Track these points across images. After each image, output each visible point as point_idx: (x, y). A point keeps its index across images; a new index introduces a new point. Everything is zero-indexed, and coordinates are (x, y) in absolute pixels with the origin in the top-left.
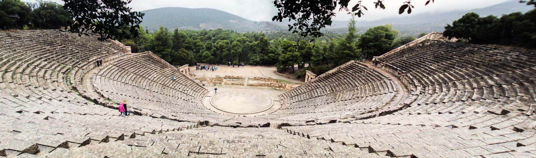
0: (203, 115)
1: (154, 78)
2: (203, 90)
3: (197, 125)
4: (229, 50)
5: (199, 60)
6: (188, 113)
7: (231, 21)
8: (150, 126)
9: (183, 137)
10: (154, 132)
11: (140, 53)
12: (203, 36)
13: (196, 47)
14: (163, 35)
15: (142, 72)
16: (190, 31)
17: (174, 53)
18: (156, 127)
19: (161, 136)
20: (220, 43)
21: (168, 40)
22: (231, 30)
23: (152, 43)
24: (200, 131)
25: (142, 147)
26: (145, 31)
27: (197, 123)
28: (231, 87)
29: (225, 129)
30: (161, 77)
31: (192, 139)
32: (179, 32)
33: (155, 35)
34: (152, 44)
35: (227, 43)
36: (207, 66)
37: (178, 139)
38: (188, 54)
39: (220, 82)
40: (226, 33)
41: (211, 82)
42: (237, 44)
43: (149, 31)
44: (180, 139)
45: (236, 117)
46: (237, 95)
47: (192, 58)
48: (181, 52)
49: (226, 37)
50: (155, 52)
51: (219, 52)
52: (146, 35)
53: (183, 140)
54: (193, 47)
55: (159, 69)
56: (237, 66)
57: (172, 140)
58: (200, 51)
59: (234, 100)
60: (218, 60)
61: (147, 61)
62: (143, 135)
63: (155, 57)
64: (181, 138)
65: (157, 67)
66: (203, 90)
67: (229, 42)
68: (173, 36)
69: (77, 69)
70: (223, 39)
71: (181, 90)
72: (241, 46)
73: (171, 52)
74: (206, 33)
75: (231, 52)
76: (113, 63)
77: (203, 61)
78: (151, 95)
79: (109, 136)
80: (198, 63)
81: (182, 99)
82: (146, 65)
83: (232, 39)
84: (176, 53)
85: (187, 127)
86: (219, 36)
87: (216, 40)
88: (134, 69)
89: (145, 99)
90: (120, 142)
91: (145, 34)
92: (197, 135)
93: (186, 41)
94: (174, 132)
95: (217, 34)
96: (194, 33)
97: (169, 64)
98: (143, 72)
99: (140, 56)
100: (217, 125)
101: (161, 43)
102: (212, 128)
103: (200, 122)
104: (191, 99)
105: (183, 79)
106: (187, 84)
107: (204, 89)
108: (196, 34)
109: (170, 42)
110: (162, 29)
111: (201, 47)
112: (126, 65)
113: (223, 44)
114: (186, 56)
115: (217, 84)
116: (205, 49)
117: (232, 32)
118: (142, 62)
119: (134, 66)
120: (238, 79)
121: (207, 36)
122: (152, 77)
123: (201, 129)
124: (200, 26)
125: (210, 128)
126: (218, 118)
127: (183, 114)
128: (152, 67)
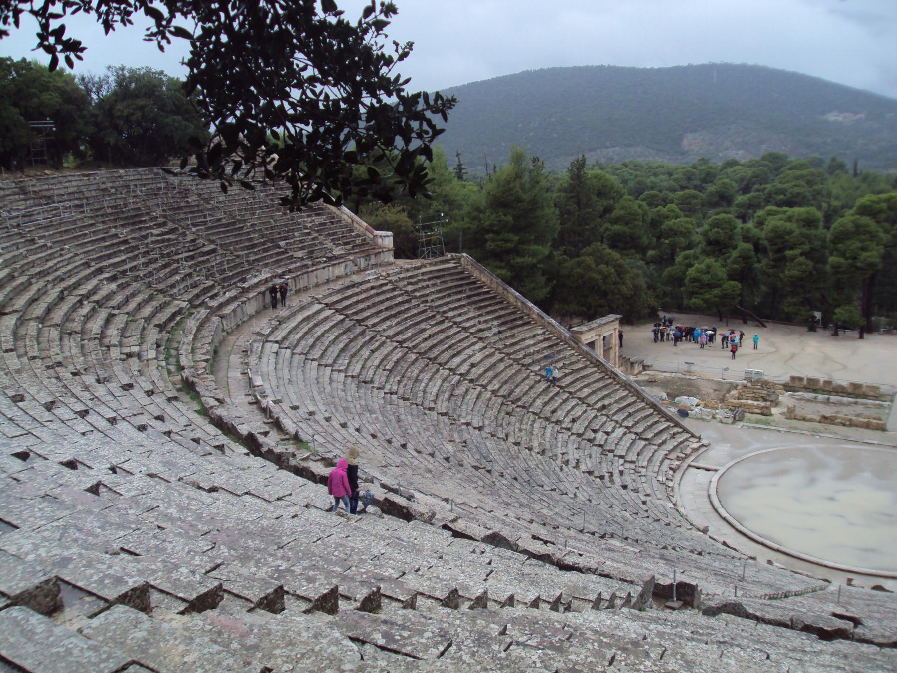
0: (670, 553)
1: (473, 366)
2: (680, 438)
3: (642, 596)
4: (815, 255)
5: (668, 299)
6: (603, 537)
7: (832, 117)
8: (441, 571)
9: (575, 641)
10: (452, 600)
11: (425, 261)
12: (695, 188)
13: (659, 238)
14: (522, 187)
15: (425, 340)
16: (637, 167)
17: (560, 263)
18: (462, 577)
19: (481, 622)
20: (773, 222)
21: (542, 208)
22: (828, 161)
23: (474, 219)
24: (652, 626)
25: (400, 657)
26: (451, 169)
27: (640, 589)
28: (815, 432)
29: (774, 639)
30: (502, 366)
31: (613, 658)
32: (590, 173)
33: (490, 187)
34: (476, 222)
35: (809, 223)
36: (703, 327)
37: (552, 646)
38: (620, 271)
39: (763, 404)
40: (804, 172)
41: (722, 400)
42: (857, 226)
43: (469, 171)
44: (560, 649)
45: (832, 588)
46: (843, 477)
47: (636, 288)
48: (589, 260)
49: (805, 190)
50: (484, 257)
51: (765, 261)
52: (455, 189)
53: (572, 657)
54: (645, 240)
55: (495, 330)
56: (856, 334)
57: (524, 645)
58: (678, 259)
59: (831, 499)
60: (758, 300)
61: (449, 295)
62: (410, 604)
63: (485, 277)
64: (566, 644)
65: (486, 321)
66: (680, 438)
67: (819, 215)
68: (564, 190)
69: (203, 312)
70: (790, 204)
71: (578, 427)
72: (881, 235)
73: (550, 257)
74: (708, 178)
75: (825, 262)
76: (325, 297)
77: (685, 301)
78: (456, 436)
79: (285, 588)
80: (665, 309)
81: (583, 467)
82: (445, 308)
83: (835, 203)
84: (570, 263)
85: (593, 597)
86: (769, 187)
87: (753, 206)
88: (398, 323)
89: (430, 449)
90: (322, 619)
91: (450, 181)
92: (636, 644)
93: (617, 213)
94: (536, 612)
95: (761, 179)
96: (655, 175)
97: (536, 309)
98: (430, 336)
99: (423, 274)
100: (735, 609)
101: (510, 218)
102: (712, 621)
103: (657, 586)
104: (621, 473)
105: (591, 379)
106: (606, 402)
107: (685, 430)
108: (663, 181)
109: (550, 214)
110: (518, 159)
111: (682, 241)
112: (369, 307)
113: (788, 225)
114: (614, 277)
115: (748, 415)
116: (698, 250)
117: (836, 167)
118: (429, 298)
119: (400, 313)
120: (857, 396)
121: (711, 188)
122: (465, 361)
123: (656, 620)
124: (685, 143)
125: (702, 620)
126: (742, 579)
127: (581, 537)
128: (468, 319)
